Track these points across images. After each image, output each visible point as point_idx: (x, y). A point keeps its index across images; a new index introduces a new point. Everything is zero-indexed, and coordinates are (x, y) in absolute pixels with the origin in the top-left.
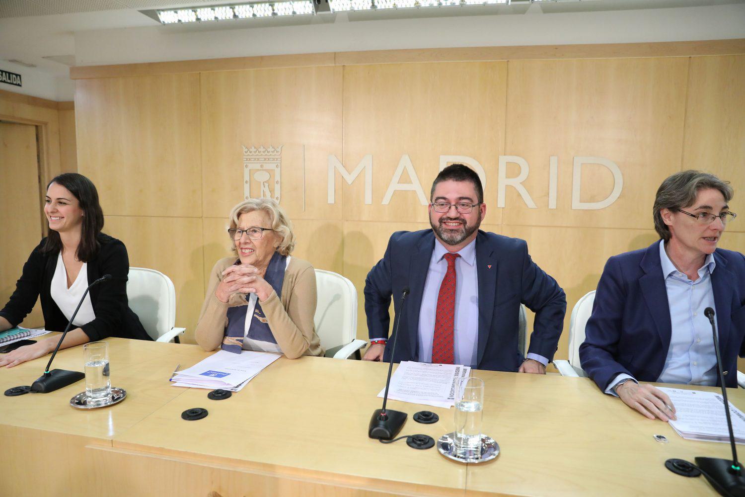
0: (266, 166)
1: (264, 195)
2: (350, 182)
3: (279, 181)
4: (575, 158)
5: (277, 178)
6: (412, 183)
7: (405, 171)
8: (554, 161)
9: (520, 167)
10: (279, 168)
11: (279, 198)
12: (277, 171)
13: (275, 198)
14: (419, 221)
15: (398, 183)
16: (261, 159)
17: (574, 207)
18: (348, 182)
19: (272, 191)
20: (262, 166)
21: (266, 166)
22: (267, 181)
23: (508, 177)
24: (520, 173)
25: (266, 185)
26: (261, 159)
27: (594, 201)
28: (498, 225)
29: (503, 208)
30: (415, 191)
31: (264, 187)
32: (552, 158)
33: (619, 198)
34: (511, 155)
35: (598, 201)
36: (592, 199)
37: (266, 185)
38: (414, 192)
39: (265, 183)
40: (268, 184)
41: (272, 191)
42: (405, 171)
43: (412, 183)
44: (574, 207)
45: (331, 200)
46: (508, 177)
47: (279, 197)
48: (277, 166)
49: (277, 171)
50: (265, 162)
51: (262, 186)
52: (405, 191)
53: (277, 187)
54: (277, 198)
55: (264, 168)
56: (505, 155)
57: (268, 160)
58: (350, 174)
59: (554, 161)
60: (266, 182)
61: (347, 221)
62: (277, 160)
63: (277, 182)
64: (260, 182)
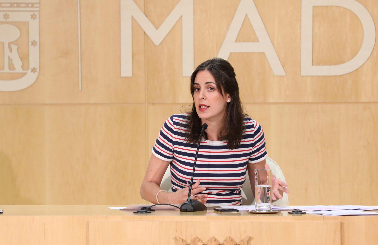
0: (15, 17)
1: (11, 67)
2: (157, 41)
3: (37, 40)
5: (34, 36)
6: (258, 41)
7: (246, 21)
10: (37, 20)
11: (38, 70)
12: (34, 25)
13: (30, 70)
14: (271, 100)
15: (236, 41)
16: (3, 5)
18: (154, 41)
19: (24, 58)
20: (6, 16)
21: (15, 17)
22: (16, 40)
25: (14, 47)
26: (3, 5)
30: (263, 53)
31: (11, 51)
37: (14, 47)
39: (12, 46)
40: (17, 47)
41: (24, 58)
42: (246, 21)
43: (258, 41)
47: (37, 67)
48: (33, 17)
49: (34, 25)
50: (10, 9)
51: (7, 50)
52: (247, 53)
53: (34, 52)
54: (34, 70)
55: (8, 20)
57: (17, 7)
58: (157, 28)
60: (12, 43)
61: (153, 104)
62: (33, 6)
63: (34, 43)
64: (3, 44)
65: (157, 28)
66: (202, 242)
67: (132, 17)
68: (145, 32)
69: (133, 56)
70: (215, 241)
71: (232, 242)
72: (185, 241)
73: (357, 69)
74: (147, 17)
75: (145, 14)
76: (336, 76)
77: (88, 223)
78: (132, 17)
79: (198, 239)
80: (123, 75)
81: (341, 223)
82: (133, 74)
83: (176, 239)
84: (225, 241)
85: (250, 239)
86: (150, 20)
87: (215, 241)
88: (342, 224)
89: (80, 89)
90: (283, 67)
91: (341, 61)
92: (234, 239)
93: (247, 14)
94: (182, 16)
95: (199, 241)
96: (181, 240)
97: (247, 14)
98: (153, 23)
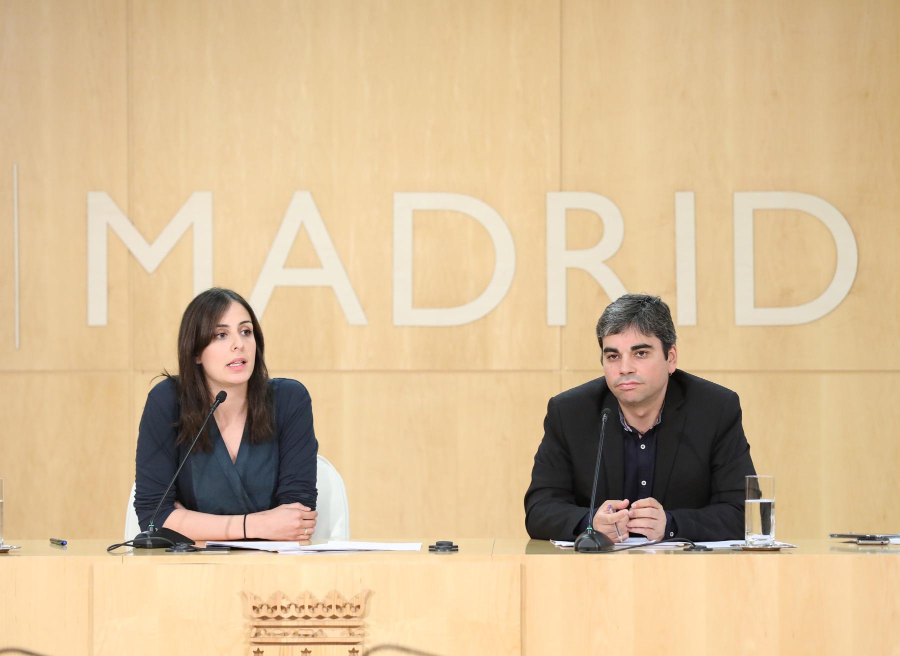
4: (738, 196)
7: (302, 233)
8: (685, 203)
9: (600, 220)
15: (284, 267)
17: (739, 322)
23: (570, 246)
24: (601, 236)
27: (788, 304)
28: (551, 371)
29: (562, 327)
32: (679, 195)
33: (850, 293)
34: (577, 189)
35: (798, 303)
36: (785, 299)
38: (328, 290)
42: (302, 233)
44: (739, 322)
45: (98, 314)
46: (570, 246)
56: (561, 190)
58: (150, 242)
59: (685, 203)
61: (143, 372)
65: (150, 242)
66: (287, 600)
67: (108, 225)
68: (129, 252)
69: (109, 289)
70: (311, 597)
71: (338, 599)
72: (260, 600)
73: (485, 317)
74: (133, 223)
75: (129, 218)
76: (450, 328)
77: (91, 569)
78: (108, 225)
79: (282, 595)
80: (92, 321)
81: (521, 566)
82: (109, 321)
83: (244, 595)
84: (327, 597)
85: (369, 594)
86: (140, 231)
87: (311, 597)
88: (522, 567)
89: (17, 346)
90: (364, 309)
91: (458, 302)
92: (342, 594)
93: (302, 225)
94: (192, 225)
95: (283, 598)
96: (253, 597)
97: (302, 225)
98: (143, 234)
